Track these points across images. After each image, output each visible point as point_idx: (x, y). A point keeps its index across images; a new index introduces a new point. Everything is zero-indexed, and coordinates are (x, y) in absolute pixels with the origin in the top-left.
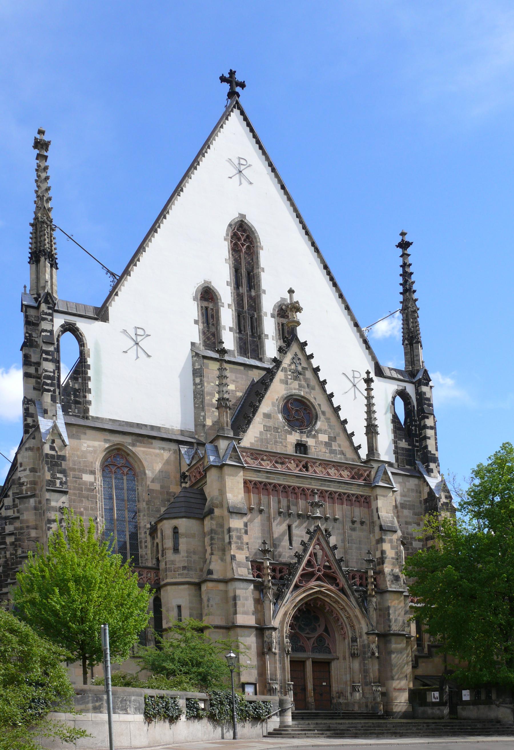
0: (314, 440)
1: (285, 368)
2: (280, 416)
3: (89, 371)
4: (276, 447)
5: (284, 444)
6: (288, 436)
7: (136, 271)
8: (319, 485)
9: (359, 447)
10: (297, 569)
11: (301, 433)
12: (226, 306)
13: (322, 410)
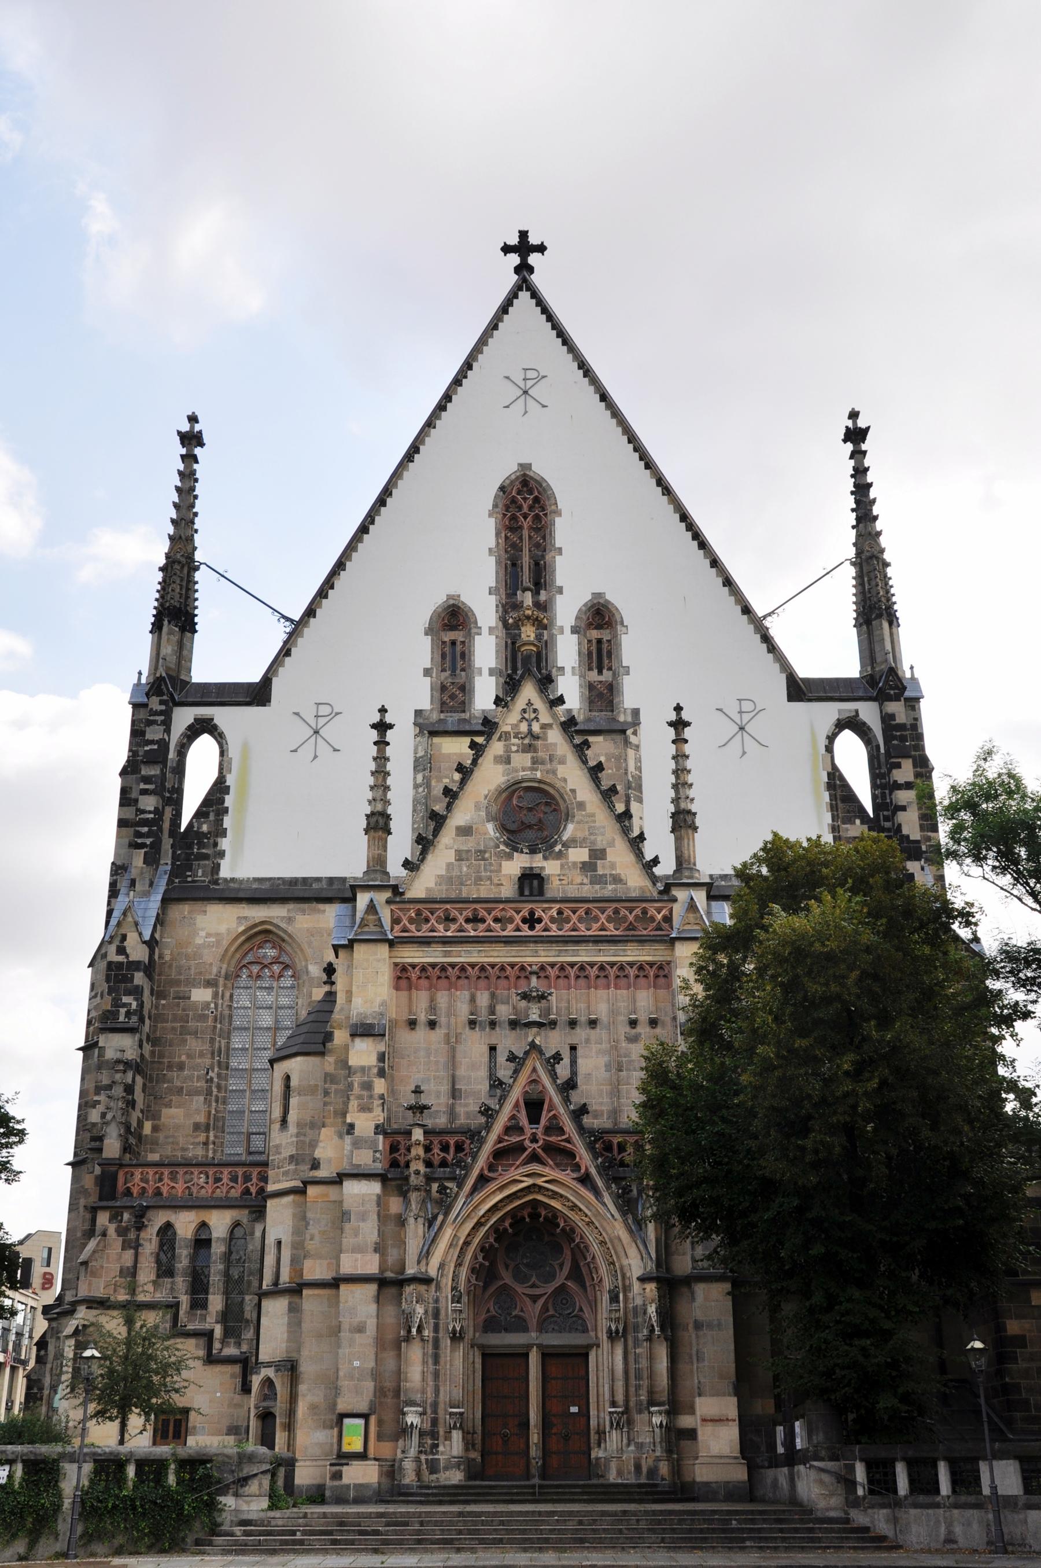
0: (558, 862)
1: (506, 733)
2: (490, 828)
3: (227, 797)
4: (478, 890)
5: (496, 881)
6: (504, 863)
8: (553, 953)
9: (656, 861)
10: (482, 1141)
11: (533, 851)
12: (485, 631)
13: (578, 799)
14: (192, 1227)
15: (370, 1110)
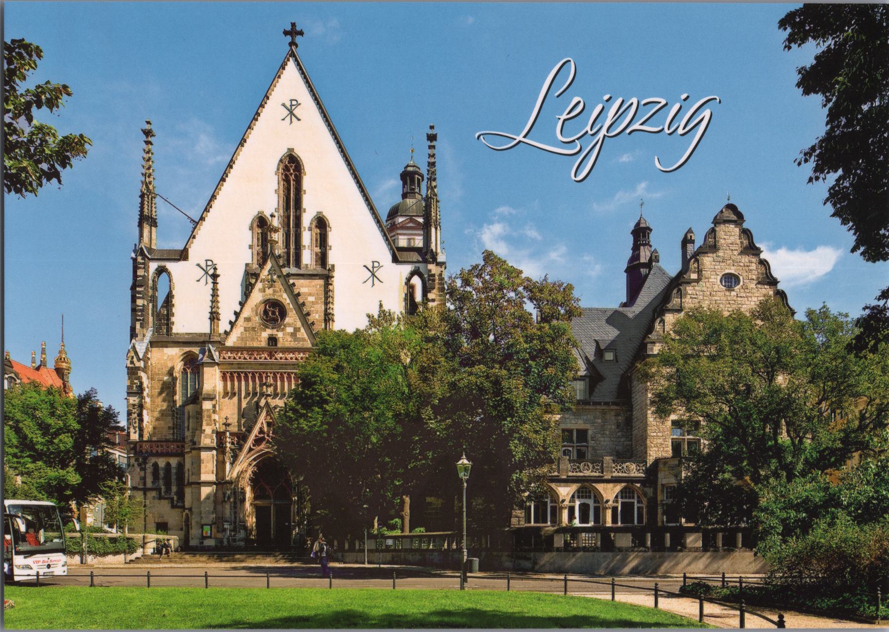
7: (210, 217)
14: (164, 463)
15: (211, 425)
